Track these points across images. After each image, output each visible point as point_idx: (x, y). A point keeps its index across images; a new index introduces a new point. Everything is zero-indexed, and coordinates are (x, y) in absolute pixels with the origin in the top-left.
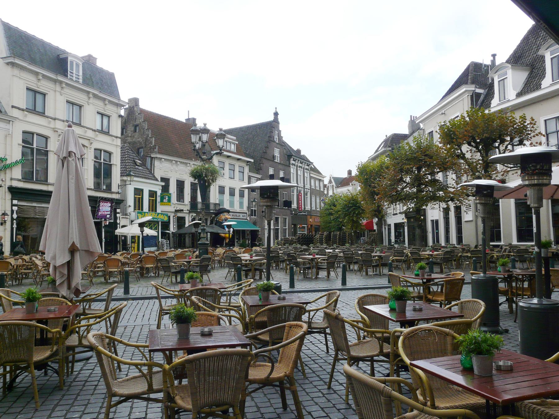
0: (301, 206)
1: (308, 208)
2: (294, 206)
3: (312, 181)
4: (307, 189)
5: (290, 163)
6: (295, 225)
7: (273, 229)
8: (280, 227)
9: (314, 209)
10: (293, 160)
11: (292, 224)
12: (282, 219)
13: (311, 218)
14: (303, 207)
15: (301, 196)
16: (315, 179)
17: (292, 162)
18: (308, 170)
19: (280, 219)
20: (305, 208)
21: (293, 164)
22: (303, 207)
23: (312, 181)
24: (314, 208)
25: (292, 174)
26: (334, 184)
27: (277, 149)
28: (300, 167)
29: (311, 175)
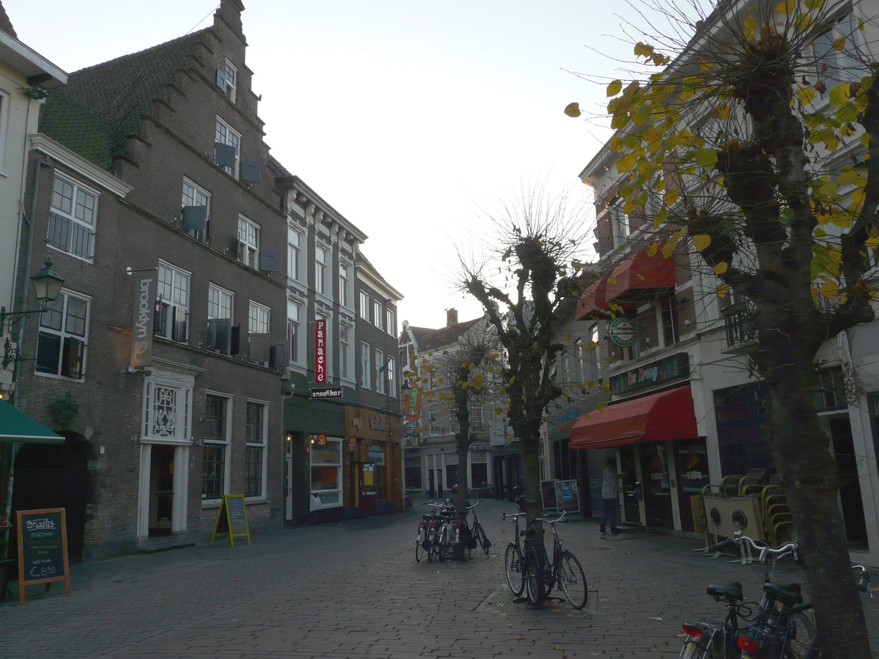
0: (324, 365)
1: (349, 378)
2: (300, 363)
3: (363, 299)
4: (344, 316)
5: (283, 206)
6: (298, 437)
7: (193, 448)
8: (228, 440)
9: (368, 387)
10: (297, 201)
11: (288, 433)
12: (243, 408)
13: (358, 416)
14: (330, 372)
15: (324, 329)
16: (373, 297)
17: (292, 206)
18: (351, 257)
19: (230, 405)
20: (337, 379)
21: (295, 215)
22: (330, 372)
23: (363, 299)
24: (367, 384)
25: (291, 254)
26: (413, 342)
27: (229, 128)
28: (322, 235)
29: (360, 276)
